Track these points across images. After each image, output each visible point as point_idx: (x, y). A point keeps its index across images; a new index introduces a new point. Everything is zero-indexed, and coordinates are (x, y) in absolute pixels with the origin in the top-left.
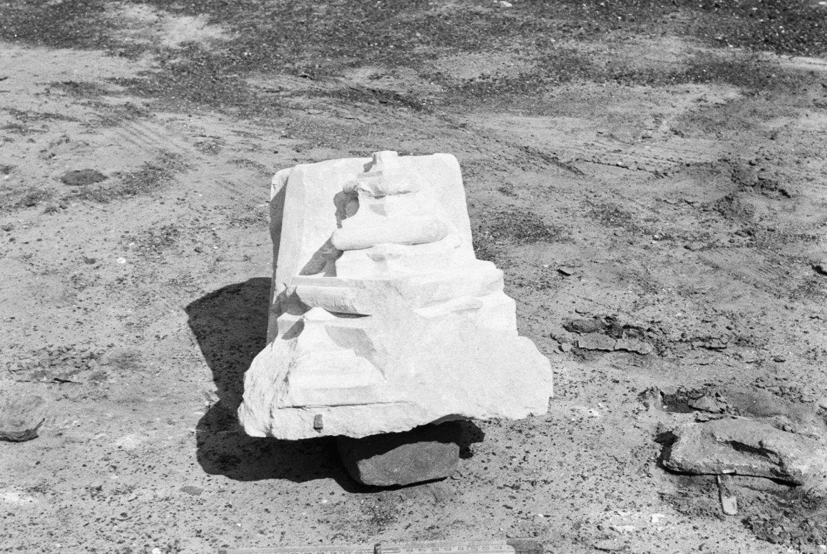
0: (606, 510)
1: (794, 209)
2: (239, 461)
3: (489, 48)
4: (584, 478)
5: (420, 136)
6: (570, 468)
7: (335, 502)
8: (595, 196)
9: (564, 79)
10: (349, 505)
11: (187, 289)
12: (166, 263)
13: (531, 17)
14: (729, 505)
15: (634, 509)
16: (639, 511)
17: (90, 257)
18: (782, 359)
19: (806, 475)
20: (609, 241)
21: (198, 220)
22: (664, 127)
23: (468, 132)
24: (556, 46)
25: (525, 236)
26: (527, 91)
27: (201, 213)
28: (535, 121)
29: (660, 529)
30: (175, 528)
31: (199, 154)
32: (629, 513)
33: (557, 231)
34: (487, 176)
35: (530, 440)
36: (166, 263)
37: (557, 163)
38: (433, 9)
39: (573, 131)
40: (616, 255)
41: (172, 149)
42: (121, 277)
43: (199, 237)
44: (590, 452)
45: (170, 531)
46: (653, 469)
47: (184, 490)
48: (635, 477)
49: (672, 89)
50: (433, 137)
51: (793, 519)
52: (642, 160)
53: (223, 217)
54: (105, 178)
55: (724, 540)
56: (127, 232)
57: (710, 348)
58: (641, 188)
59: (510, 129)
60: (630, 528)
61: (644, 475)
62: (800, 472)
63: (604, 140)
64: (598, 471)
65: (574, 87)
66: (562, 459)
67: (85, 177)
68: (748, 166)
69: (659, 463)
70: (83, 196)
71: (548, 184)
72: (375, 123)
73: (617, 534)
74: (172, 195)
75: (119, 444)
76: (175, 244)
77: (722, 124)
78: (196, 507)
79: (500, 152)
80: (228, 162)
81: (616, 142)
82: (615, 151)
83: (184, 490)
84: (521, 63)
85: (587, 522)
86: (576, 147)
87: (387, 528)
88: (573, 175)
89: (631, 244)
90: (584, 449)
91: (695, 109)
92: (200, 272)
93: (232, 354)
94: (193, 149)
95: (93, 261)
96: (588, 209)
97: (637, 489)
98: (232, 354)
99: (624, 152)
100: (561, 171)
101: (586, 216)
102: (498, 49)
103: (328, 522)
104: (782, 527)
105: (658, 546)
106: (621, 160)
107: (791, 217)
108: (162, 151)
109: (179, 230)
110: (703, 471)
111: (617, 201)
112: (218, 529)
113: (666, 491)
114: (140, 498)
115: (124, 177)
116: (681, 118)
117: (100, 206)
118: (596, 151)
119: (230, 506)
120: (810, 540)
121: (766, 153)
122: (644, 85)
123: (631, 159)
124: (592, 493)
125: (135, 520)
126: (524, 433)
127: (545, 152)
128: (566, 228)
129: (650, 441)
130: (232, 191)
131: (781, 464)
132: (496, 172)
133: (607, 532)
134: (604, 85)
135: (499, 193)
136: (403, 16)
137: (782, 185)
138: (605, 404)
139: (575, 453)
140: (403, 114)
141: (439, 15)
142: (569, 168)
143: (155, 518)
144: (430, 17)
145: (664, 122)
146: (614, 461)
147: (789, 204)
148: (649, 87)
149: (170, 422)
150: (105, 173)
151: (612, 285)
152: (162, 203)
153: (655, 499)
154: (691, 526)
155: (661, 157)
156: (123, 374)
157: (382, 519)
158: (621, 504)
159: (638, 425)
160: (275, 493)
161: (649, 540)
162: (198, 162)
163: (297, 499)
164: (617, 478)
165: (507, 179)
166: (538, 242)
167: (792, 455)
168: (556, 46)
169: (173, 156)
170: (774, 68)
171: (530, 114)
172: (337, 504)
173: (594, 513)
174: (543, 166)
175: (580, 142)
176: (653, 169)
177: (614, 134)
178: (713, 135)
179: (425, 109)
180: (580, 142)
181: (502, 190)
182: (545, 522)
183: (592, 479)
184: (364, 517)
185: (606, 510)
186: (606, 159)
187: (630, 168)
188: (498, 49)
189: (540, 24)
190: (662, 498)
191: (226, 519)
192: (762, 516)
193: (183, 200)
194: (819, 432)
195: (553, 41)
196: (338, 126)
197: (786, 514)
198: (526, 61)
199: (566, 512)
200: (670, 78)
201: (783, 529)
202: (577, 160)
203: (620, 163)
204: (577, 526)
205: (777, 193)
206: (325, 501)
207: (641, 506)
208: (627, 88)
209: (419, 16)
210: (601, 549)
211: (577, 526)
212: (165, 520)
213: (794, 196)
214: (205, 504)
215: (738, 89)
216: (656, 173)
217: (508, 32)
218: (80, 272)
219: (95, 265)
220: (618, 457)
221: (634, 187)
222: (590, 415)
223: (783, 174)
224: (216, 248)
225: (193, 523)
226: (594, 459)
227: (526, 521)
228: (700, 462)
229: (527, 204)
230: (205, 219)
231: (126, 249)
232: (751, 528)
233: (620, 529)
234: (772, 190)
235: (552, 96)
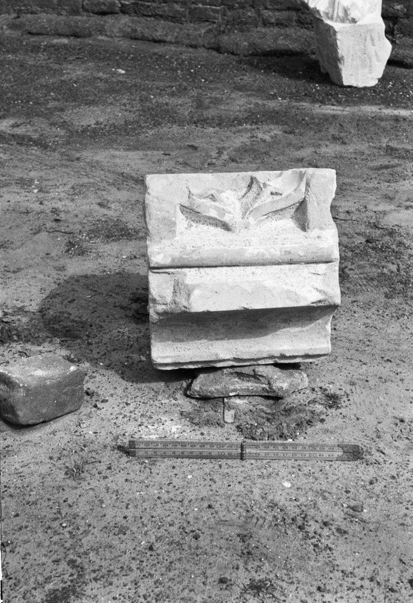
0: (140, 425)
3: (105, 103)
9: (157, 124)
13: (138, 80)
14: (229, 416)
19: (287, 391)
24: (154, 101)
25: (112, 236)
26: (128, 133)
28: (131, 154)
29: (176, 436)
33: (137, 232)
34: (90, 194)
35: (92, 380)
38: (65, 76)
39: (158, 161)
51: (273, 423)
59: (113, 161)
62: (282, 388)
64: (138, 399)
65: (164, 130)
79: (103, 177)
84: (127, 114)
85: (124, 435)
102: (111, 104)
104: (263, 428)
110: (216, 395)
120: (281, 437)
131: (269, 384)
132: (97, 191)
136: (43, 81)
141: (70, 80)
144: (62, 81)
154: (199, 432)
164: (152, 402)
168: (154, 101)
171: (129, 150)
173: (131, 428)
177: (188, 162)
182: (93, 436)
185: (140, 425)
188: (111, 104)
189: (144, 85)
192: (250, 422)
195: (152, 97)
197: (268, 420)
198: (130, 111)
201: (263, 430)
209: (55, 80)
217: (120, 91)
227: (79, 438)
228: (212, 389)
229: (118, 213)
232: (242, 431)
235: (147, 137)
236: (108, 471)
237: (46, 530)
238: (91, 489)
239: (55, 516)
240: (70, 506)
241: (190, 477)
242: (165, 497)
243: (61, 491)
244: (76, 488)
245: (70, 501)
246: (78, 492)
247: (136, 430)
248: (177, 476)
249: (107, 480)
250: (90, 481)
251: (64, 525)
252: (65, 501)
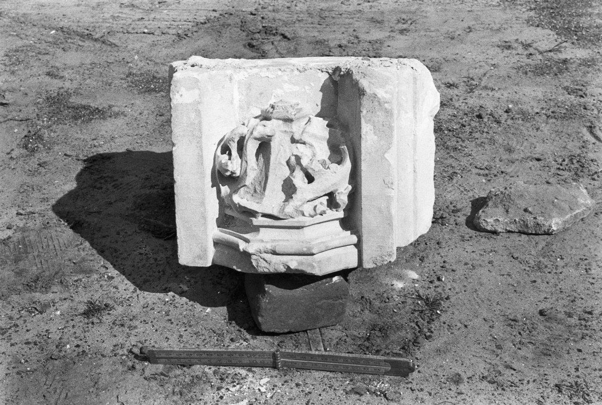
23: (5, 20)
34: (32, 62)
52: (163, 25)
63: (126, 10)
71: (88, 61)
79: (38, 36)
81: (138, 11)
82: (139, 20)
88: (109, 48)
99: (146, 18)
100: (98, 45)
111: (151, 67)
132: (40, 57)
135: (47, 77)
137: (283, 30)
142: (104, 42)
165: (51, 62)
166: (93, 121)
174: (81, 43)
176: (174, 31)
180: (107, 16)
181: (48, 74)
186: (133, 29)
187: (156, 33)
202: (109, 33)
203: (146, 31)
205: (279, 38)
213: (293, 38)
216: (179, 35)
221: (165, 52)
223: (279, 19)
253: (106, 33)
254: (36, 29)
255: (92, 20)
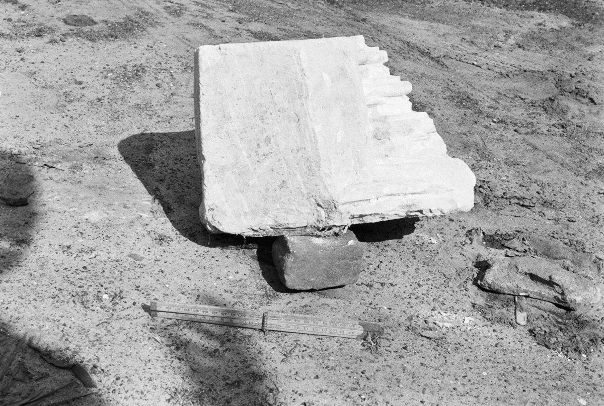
0: (433, 310)
1: (598, 113)
2: (172, 240)
4: (419, 285)
5: (331, 24)
6: (410, 277)
7: (238, 280)
8: (454, 85)
10: (248, 283)
11: (147, 112)
12: (134, 92)
14: (521, 318)
15: (452, 312)
16: (456, 314)
17: (78, 79)
18: (574, 220)
19: (579, 304)
20: (459, 119)
21: (161, 64)
22: (512, 41)
27: (164, 59)
28: (416, 23)
29: (469, 328)
30: (121, 282)
31: (166, 15)
32: (448, 314)
35: (384, 254)
36: (134, 92)
37: (429, 57)
39: (444, 35)
40: (464, 129)
41: (147, 9)
42: (100, 97)
43: (161, 76)
44: (426, 267)
45: (117, 284)
46: (470, 285)
47: (130, 256)
48: (456, 289)
49: (521, 13)
50: (341, 25)
51: (566, 334)
52: (492, 63)
53: (180, 64)
54: (96, 23)
55: (514, 342)
56: (108, 65)
57: (523, 206)
58: (487, 83)
59: (398, 27)
60: (448, 325)
61: (463, 289)
62: (576, 301)
63: (465, 44)
64: (430, 282)
66: (405, 270)
67: (81, 21)
68: (569, 78)
69: (475, 282)
70: (78, 35)
71: (421, 72)
72: (299, 10)
73: (438, 328)
74: (144, 43)
75: (86, 217)
76: (142, 79)
77: (554, 44)
78: (138, 269)
79: (389, 43)
80: (188, 24)
82: (473, 54)
83: (130, 256)
85: (418, 317)
86: (445, 47)
87: (273, 302)
88: (440, 67)
89: (476, 123)
90: (422, 265)
91: (536, 30)
92: (158, 102)
93: (176, 164)
94: (162, 10)
95: (80, 83)
96: (448, 94)
97: (457, 298)
98: (176, 164)
99: (479, 54)
100: (432, 63)
101: (445, 99)
103: (231, 292)
104: (557, 338)
105: (466, 340)
106: (477, 61)
107: (595, 119)
108: (140, 9)
109: (146, 69)
110: (506, 292)
111: (469, 90)
112: (151, 287)
113: (477, 302)
114: (98, 257)
115: (109, 25)
116: (525, 36)
117: (90, 44)
118: (459, 52)
119: (163, 272)
120: (575, 350)
121: (583, 70)
122: (501, 8)
123: (484, 61)
124: (424, 296)
125: (93, 272)
126: (380, 248)
127: (421, 47)
128: (430, 105)
129: (470, 265)
130: (189, 45)
131: (563, 294)
133: (431, 325)
134: (472, 4)
138: (442, 235)
139: (415, 267)
140: (320, 6)
142: (438, 62)
143: (107, 274)
145: (512, 37)
146: (442, 276)
147: (595, 109)
148: (504, 10)
149: (125, 207)
150: (96, 19)
151: (458, 152)
152: (136, 48)
153: (468, 306)
154: (492, 329)
155: (506, 62)
156: (95, 167)
157: (270, 296)
158: (445, 307)
159: (463, 253)
160: (196, 267)
161: (461, 335)
162: (166, 21)
163: (211, 273)
164: (443, 288)
167: (571, 288)
169: (147, 14)
170: (598, 8)
171: (414, 18)
172: (240, 281)
173: (424, 311)
174: (419, 57)
175: (449, 44)
176: (499, 71)
177: (474, 41)
178: (547, 51)
179: (338, 4)
180: (449, 44)
182: (387, 312)
183: (425, 288)
184: (257, 292)
185: (433, 310)
186: (466, 59)
187: (482, 67)
190: (474, 306)
191: (158, 280)
192: (544, 329)
193: (151, 47)
194: (592, 275)
196: (272, 8)
197: (561, 329)
199: (404, 307)
200: (521, 5)
201: (557, 339)
202: (444, 56)
203: (475, 63)
204: (410, 319)
205: (587, 100)
206: (231, 277)
207: (458, 310)
208: (488, 8)
210: (425, 337)
211: (410, 319)
212: (115, 276)
214: (144, 268)
215: (570, 20)
216: (501, 74)
218: (70, 90)
219: (81, 86)
220: (446, 274)
221: (484, 82)
222: (430, 241)
224: (172, 85)
225: (134, 280)
226: (428, 273)
227: (374, 310)
228: (504, 285)
230: (166, 63)
231: (106, 77)
232: (535, 336)
233: (441, 324)
234: (584, 97)
236: (404, 351)
237: (345, 398)
238: (388, 366)
239: (354, 386)
240: (368, 379)
241: (485, 373)
242: (461, 389)
243: (359, 362)
244: (373, 362)
245: (367, 374)
246: (376, 366)
247: (429, 313)
248: (472, 371)
249: (403, 359)
250: (386, 358)
251: (363, 397)
252: (362, 373)
253: (442, 56)
254: (388, 38)
255: (435, 44)
